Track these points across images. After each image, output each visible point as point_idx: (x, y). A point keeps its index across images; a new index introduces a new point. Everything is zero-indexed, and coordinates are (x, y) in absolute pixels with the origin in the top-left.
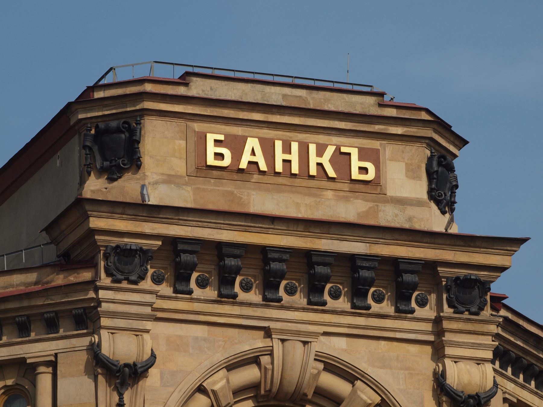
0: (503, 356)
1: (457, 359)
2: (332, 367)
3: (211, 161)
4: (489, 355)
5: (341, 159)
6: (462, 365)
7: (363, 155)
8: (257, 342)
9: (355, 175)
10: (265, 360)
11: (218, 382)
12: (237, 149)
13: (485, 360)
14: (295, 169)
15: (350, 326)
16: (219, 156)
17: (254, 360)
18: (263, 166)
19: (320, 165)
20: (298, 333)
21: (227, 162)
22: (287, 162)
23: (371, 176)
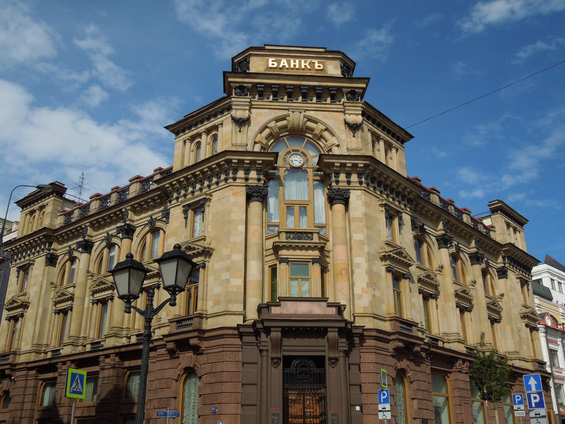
0: (363, 114)
1: (350, 114)
2: (309, 120)
3: (270, 66)
4: (360, 113)
5: (312, 64)
6: (351, 116)
7: (319, 63)
8: (285, 112)
9: (316, 67)
10: (287, 118)
11: (272, 124)
12: (279, 63)
13: (359, 114)
14: (297, 67)
15: (315, 107)
16: (273, 64)
17: (283, 118)
18: (287, 66)
19: (305, 66)
20: (298, 109)
21: (275, 66)
22: (295, 65)
23: (321, 68)
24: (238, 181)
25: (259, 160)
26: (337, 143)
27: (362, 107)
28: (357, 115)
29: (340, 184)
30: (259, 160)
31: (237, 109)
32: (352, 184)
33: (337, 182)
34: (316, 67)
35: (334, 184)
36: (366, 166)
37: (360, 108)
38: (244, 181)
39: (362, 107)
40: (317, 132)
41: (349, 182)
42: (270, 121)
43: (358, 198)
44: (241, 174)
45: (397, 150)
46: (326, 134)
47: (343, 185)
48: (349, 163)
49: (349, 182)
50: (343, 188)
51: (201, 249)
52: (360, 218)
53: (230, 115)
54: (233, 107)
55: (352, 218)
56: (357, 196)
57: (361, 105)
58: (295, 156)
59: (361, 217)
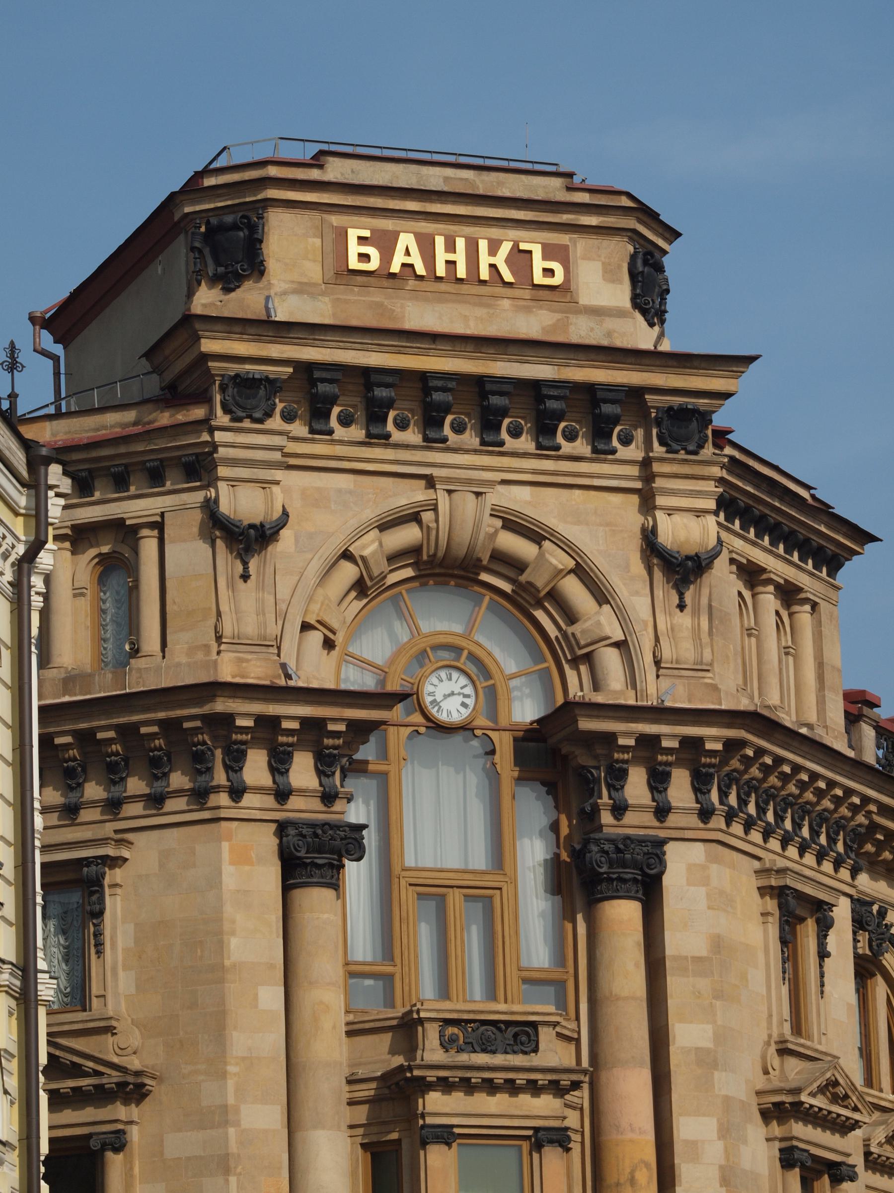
9: (539, 278)
15: (535, 472)
23: (558, 279)
24: (249, 799)
25: (335, 720)
26: (619, 636)
27: (721, 481)
28: (699, 513)
29: (630, 818)
30: (335, 720)
31: (234, 482)
32: (673, 819)
33: (619, 809)
34: (539, 278)
35: (606, 818)
36: (732, 746)
37: (710, 486)
38: (270, 801)
39: (721, 481)
40: (541, 580)
41: (662, 811)
42: (361, 533)
43: (698, 876)
44: (256, 768)
45: (814, 606)
46: (573, 589)
47: (639, 822)
48: (670, 734)
49: (662, 811)
50: (642, 832)
51: (115, 1076)
52: (697, 960)
53: (199, 497)
54: (222, 471)
55: (676, 958)
56: (690, 867)
57: (716, 471)
58: (443, 674)
59: (704, 953)
